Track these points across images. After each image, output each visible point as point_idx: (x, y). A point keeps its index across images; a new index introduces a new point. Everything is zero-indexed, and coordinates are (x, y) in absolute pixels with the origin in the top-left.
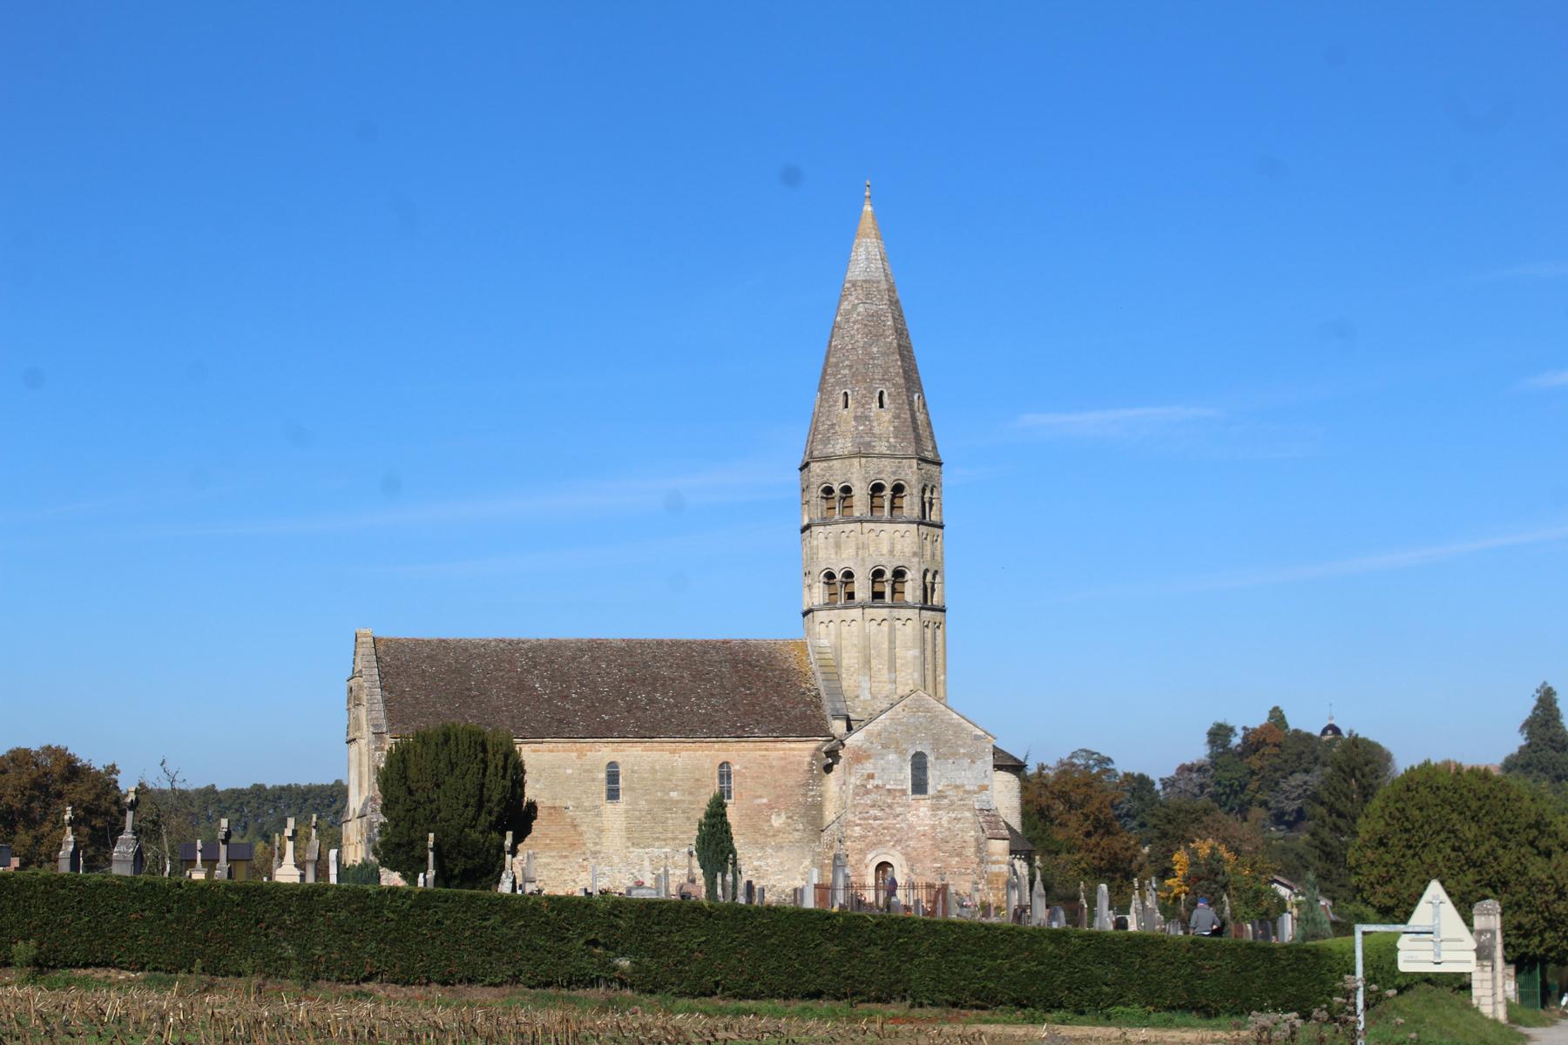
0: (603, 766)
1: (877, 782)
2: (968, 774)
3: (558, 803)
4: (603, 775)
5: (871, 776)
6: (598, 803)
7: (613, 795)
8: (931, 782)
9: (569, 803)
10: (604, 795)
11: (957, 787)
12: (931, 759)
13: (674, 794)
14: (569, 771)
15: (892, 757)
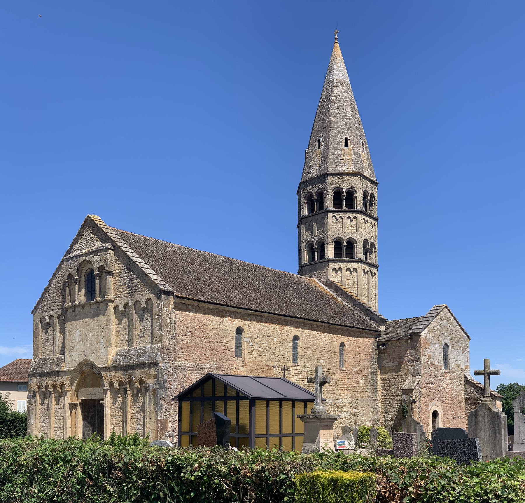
0: (291, 338)
1: (432, 360)
2: (462, 359)
3: (270, 363)
4: (291, 345)
5: (430, 357)
6: (289, 364)
7: (295, 359)
8: (451, 361)
9: (275, 364)
10: (292, 359)
11: (458, 366)
12: (450, 348)
13: (322, 361)
14: (275, 339)
15: (437, 345)
